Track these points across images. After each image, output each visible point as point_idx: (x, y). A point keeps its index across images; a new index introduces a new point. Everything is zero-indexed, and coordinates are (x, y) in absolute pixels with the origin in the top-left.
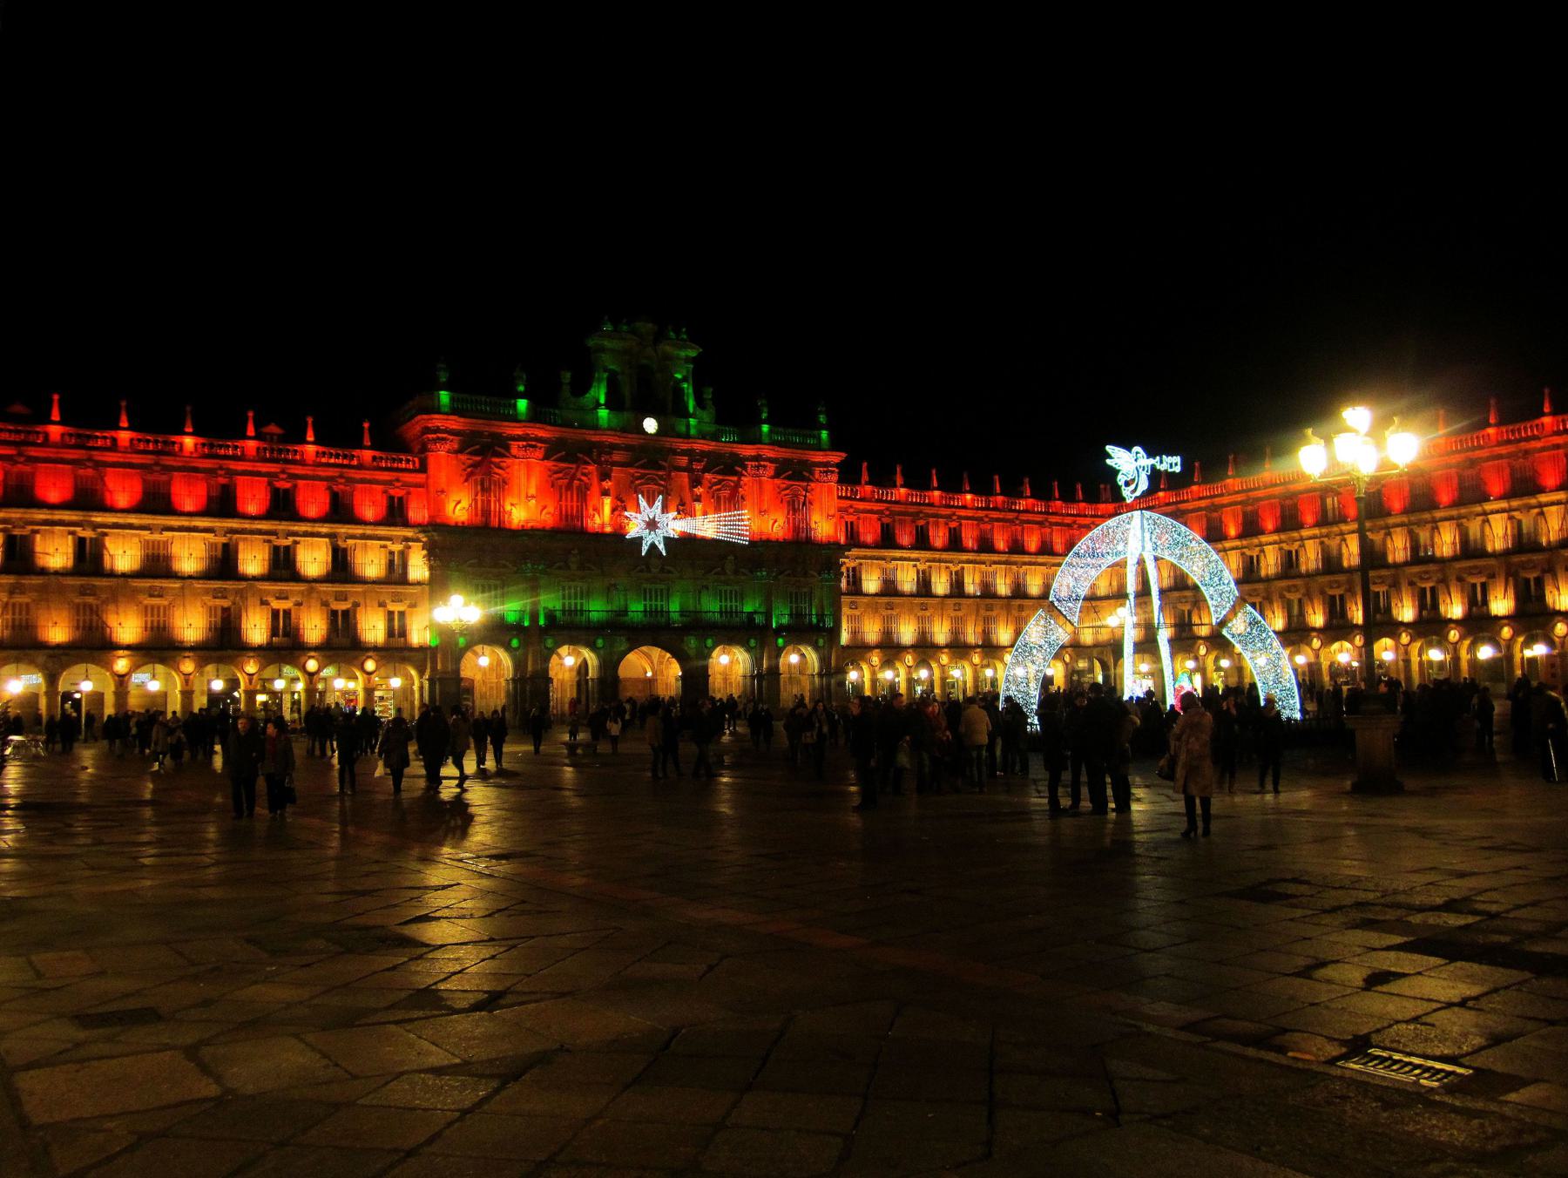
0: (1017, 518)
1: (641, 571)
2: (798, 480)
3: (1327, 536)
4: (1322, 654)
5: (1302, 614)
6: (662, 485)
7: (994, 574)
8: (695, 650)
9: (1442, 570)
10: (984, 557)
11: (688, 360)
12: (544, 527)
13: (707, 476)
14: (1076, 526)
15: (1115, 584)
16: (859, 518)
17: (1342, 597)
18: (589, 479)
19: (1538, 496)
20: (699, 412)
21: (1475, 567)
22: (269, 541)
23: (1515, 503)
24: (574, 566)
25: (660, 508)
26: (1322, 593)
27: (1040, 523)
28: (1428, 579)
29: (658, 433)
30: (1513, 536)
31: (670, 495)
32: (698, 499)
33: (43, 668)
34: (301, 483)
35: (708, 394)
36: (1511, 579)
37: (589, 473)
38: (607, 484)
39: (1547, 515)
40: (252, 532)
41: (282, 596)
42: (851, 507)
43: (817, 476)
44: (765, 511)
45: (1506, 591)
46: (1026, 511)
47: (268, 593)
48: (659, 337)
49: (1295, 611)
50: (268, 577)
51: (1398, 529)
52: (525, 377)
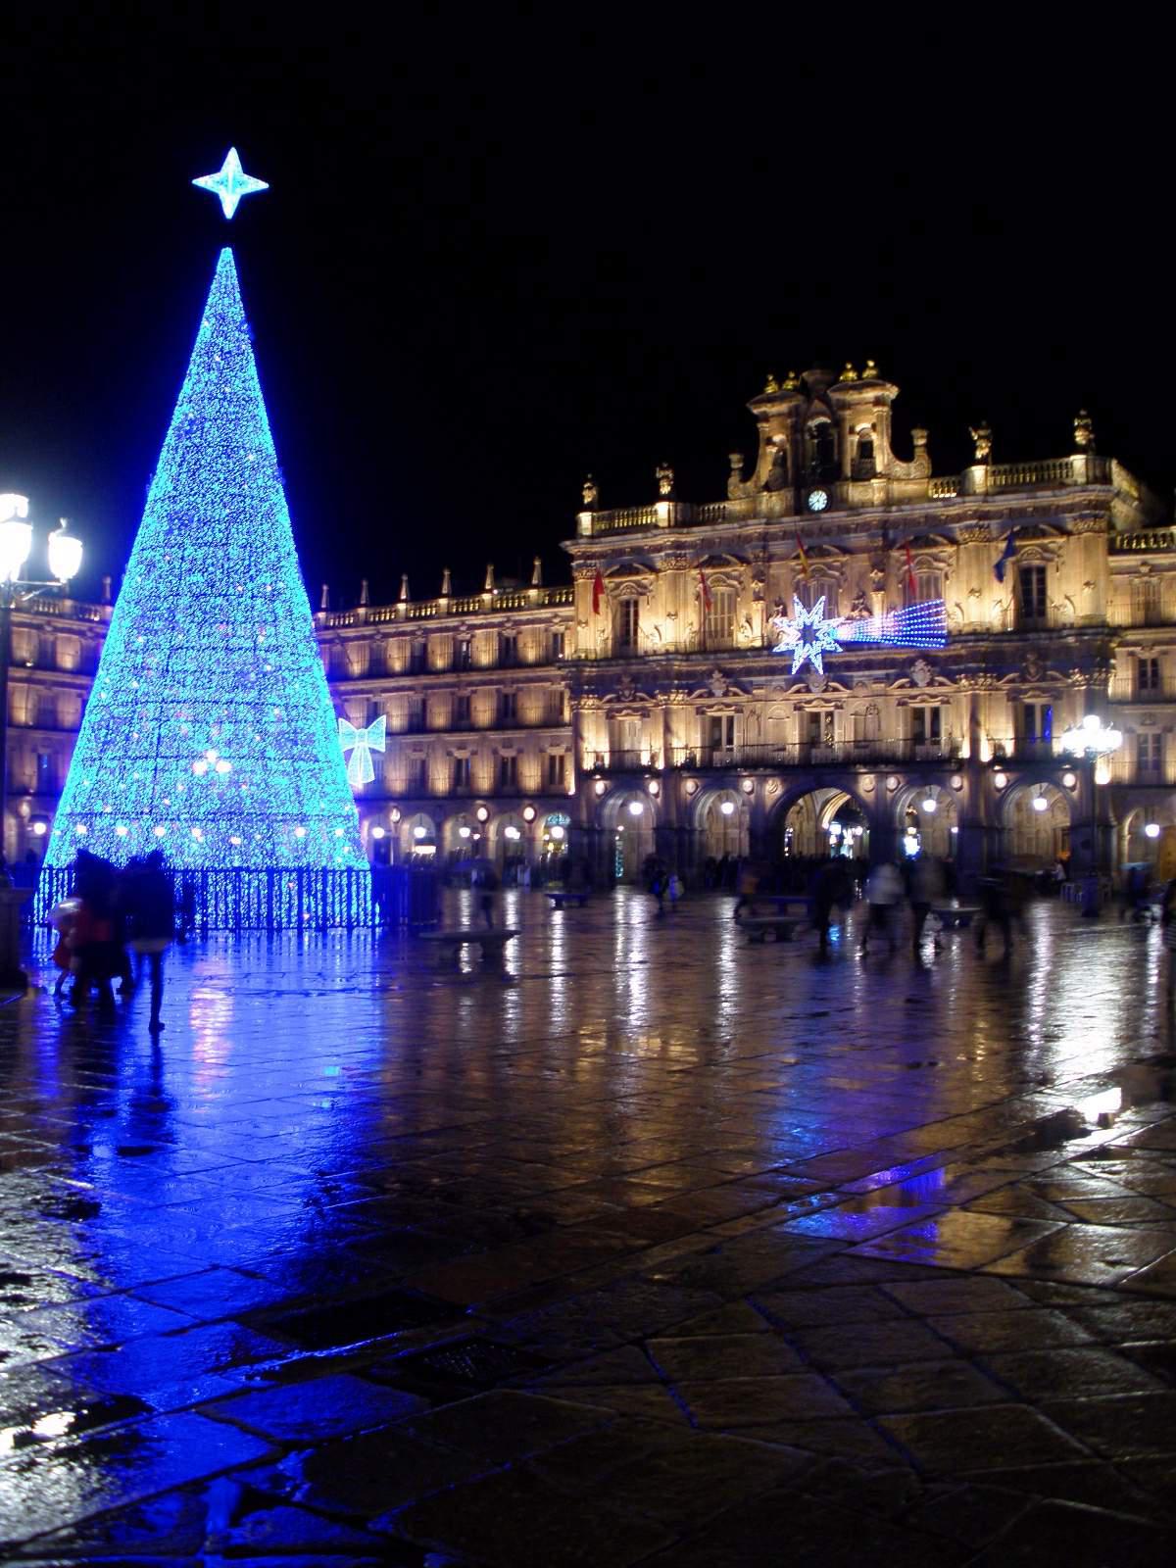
1: (798, 691)
2: (1035, 536)
6: (833, 577)
8: (873, 793)
11: (878, 402)
12: (988, 629)
13: (895, 554)
16: (1161, 579)
18: (740, 583)
20: (900, 468)
22: (453, 694)
24: (719, 692)
25: (821, 612)
29: (827, 509)
31: (840, 587)
32: (880, 587)
33: (433, 815)
34: (478, 632)
35: (920, 440)
37: (741, 575)
38: (757, 586)
40: (440, 686)
41: (461, 746)
42: (1144, 564)
43: (1070, 526)
44: (972, 591)
47: (451, 743)
48: (833, 382)
50: (454, 727)
52: (671, 475)
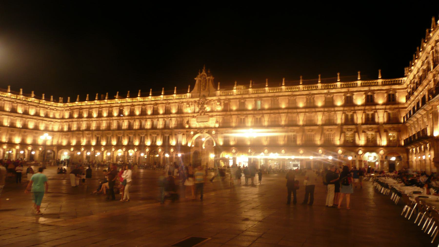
0: (27, 103)
3: (119, 120)
4: (115, 153)
5: (111, 141)
7: (16, 120)
9: (147, 132)
10: (12, 114)
14: (49, 109)
15: (60, 128)
17: (121, 137)
19: (171, 115)
21: (155, 132)
23: (165, 116)
26: (117, 135)
27: (36, 106)
28: (143, 134)
30: (164, 125)
36: (162, 136)
39: (172, 120)
45: (161, 139)
46: (31, 102)
49: (109, 140)
51: (137, 120)
